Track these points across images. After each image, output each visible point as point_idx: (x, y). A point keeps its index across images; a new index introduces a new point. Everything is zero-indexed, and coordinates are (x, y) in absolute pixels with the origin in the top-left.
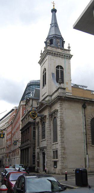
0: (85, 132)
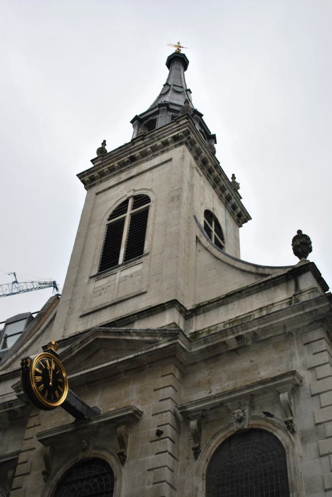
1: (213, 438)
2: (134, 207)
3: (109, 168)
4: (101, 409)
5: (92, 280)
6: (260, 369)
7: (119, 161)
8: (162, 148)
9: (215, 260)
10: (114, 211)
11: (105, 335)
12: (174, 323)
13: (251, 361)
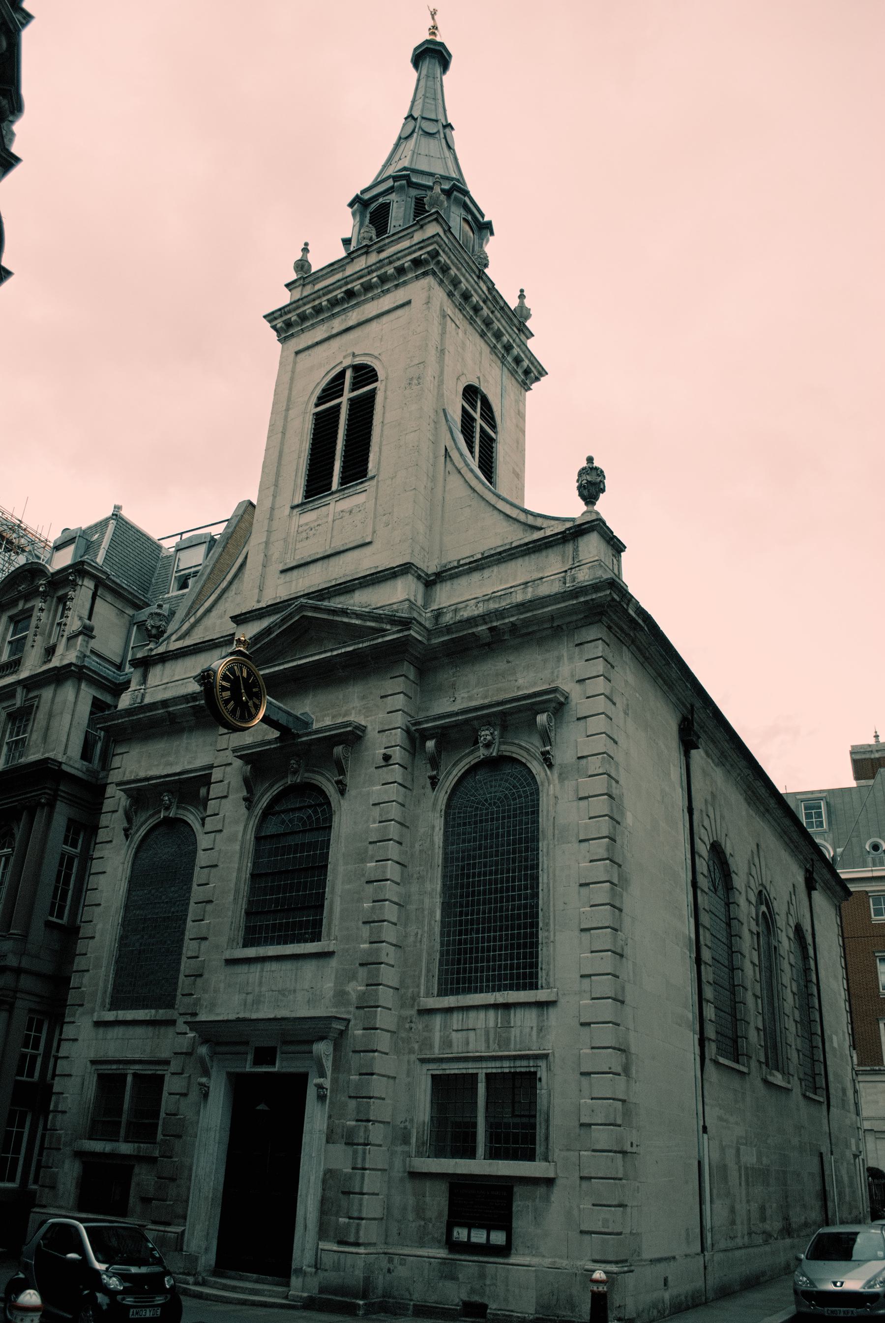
0: (693, 936)
1: (455, 765)
2: (355, 387)
3: (313, 308)
4: (312, 716)
5: (295, 511)
6: (518, 675)
7: (330, 296)
8: (395, 278)
9: (469, 492)
10: (324, 391)
11: (314, 612)
12: (409, 600)
13: (508, 662)
